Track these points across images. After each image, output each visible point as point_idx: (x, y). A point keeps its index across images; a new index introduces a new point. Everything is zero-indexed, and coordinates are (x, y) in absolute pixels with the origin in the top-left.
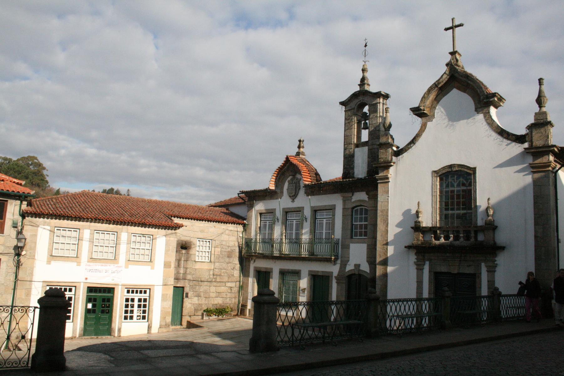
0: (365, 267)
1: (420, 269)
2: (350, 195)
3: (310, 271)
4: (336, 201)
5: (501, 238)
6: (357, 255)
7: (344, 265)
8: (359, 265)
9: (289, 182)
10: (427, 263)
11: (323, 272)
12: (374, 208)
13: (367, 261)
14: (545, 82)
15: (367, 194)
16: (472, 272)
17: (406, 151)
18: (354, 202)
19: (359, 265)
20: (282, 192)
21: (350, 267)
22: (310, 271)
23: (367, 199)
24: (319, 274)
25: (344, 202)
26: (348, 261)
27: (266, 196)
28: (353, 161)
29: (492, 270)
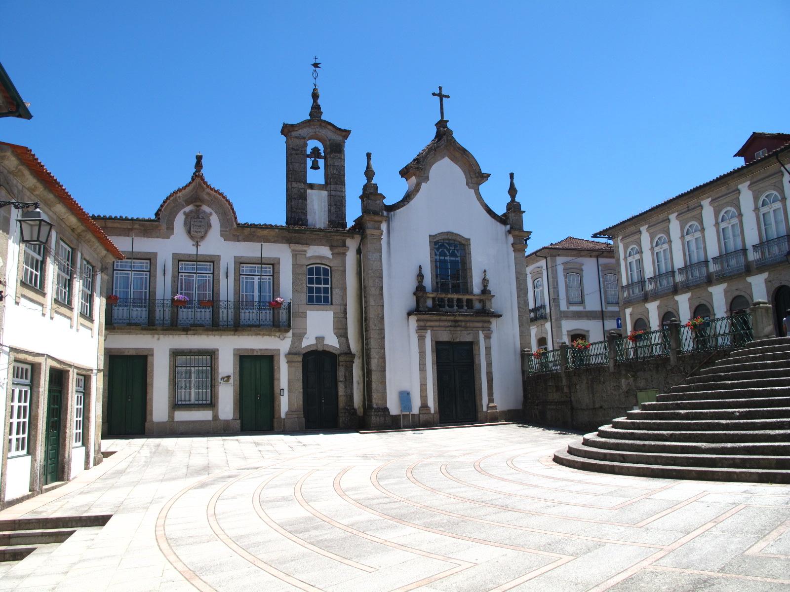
0: (332, 342)
1: (421, 339)
2: (304, 248)
3: (236, 351)
4: (282, 253)
5: (494, 306)
6: (319, 327)
7: (299, 337)
8: (323, 338)
9: (185, 213)
10: (429, 332)
11: (261, 350)
12: (342, 268)
13: (335, 334)
14: (515, 176)
15: (331, 249)
16: (471, 340)
17: (399, 208)
18: (310, 258)
19: (323, 338)
20: (170, 229)
21: (308, 342)
22: (236, 351)
23: (330, 256)
24: (255, 354)
25: (295, 256)
26: (306, 333)
27: (132, 229)
28: (306, 205)
29: (488, 337)
